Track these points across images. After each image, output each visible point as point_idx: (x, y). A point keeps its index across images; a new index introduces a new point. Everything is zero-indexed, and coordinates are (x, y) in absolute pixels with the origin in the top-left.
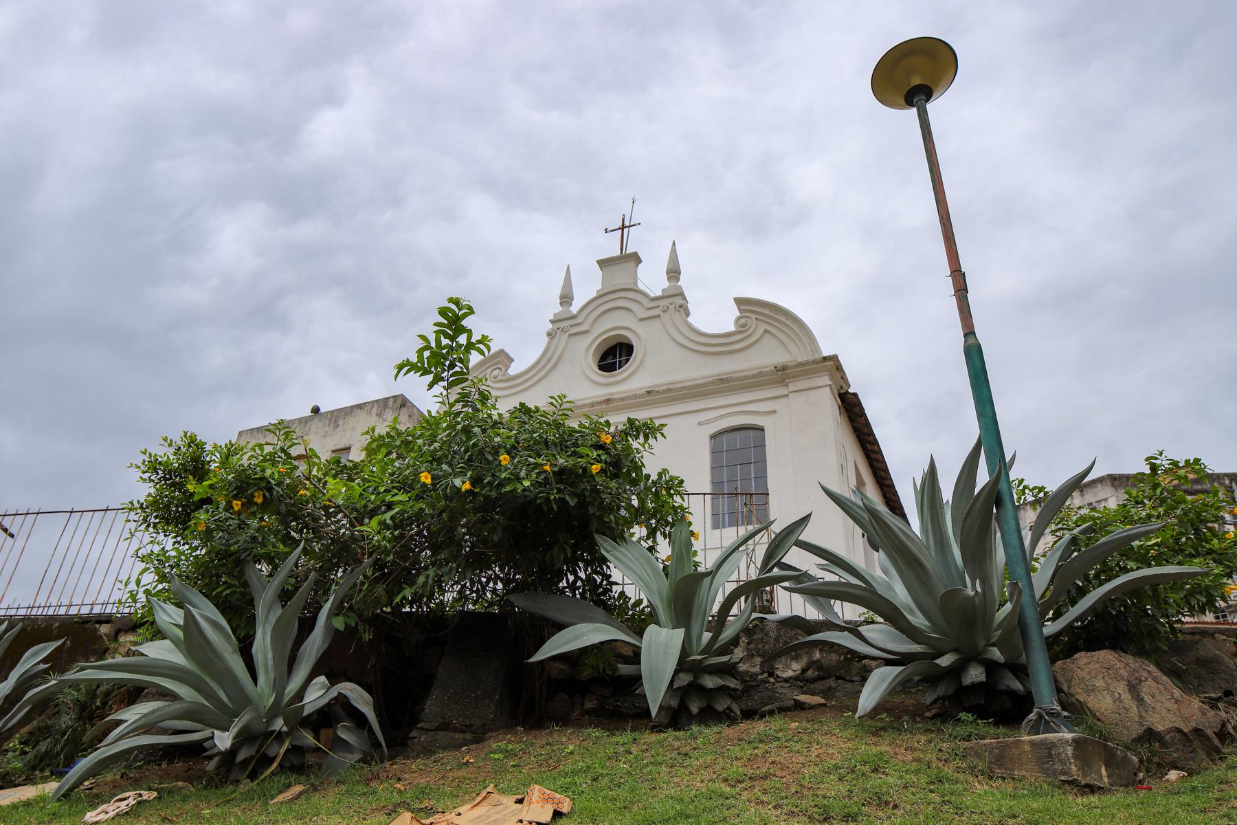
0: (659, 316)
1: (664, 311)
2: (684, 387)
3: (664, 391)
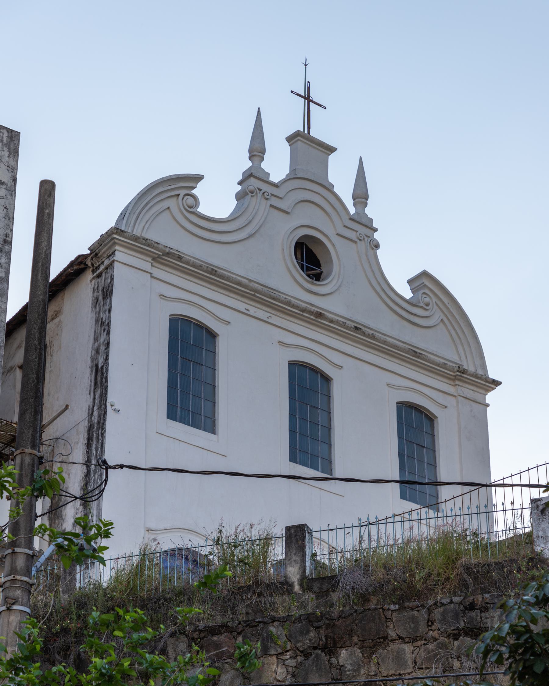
1: (360, 240)
2: (385, 341)
3: (369, 335)
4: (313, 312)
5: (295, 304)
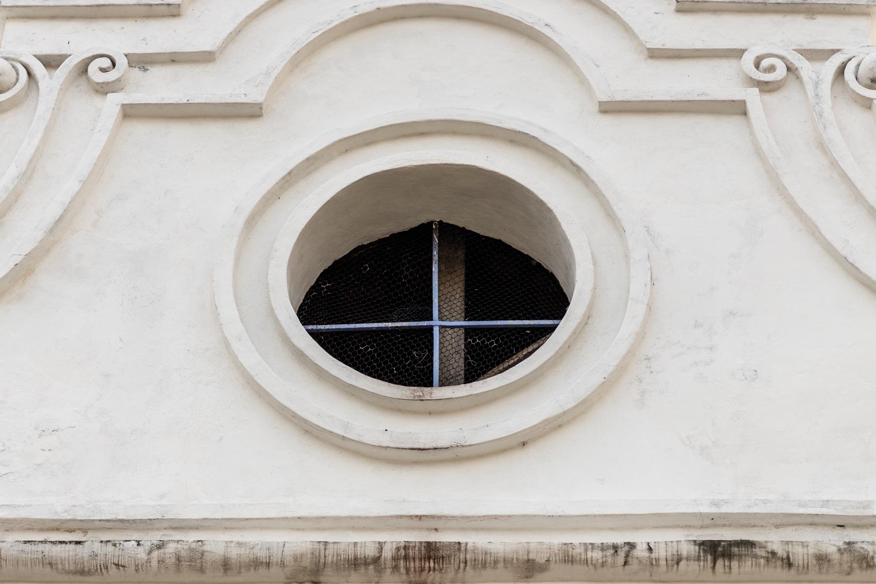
0: (739, 109)
1: (766, 87)
3: (822, 559)
4: (376, 560)
5: (234, 553)
